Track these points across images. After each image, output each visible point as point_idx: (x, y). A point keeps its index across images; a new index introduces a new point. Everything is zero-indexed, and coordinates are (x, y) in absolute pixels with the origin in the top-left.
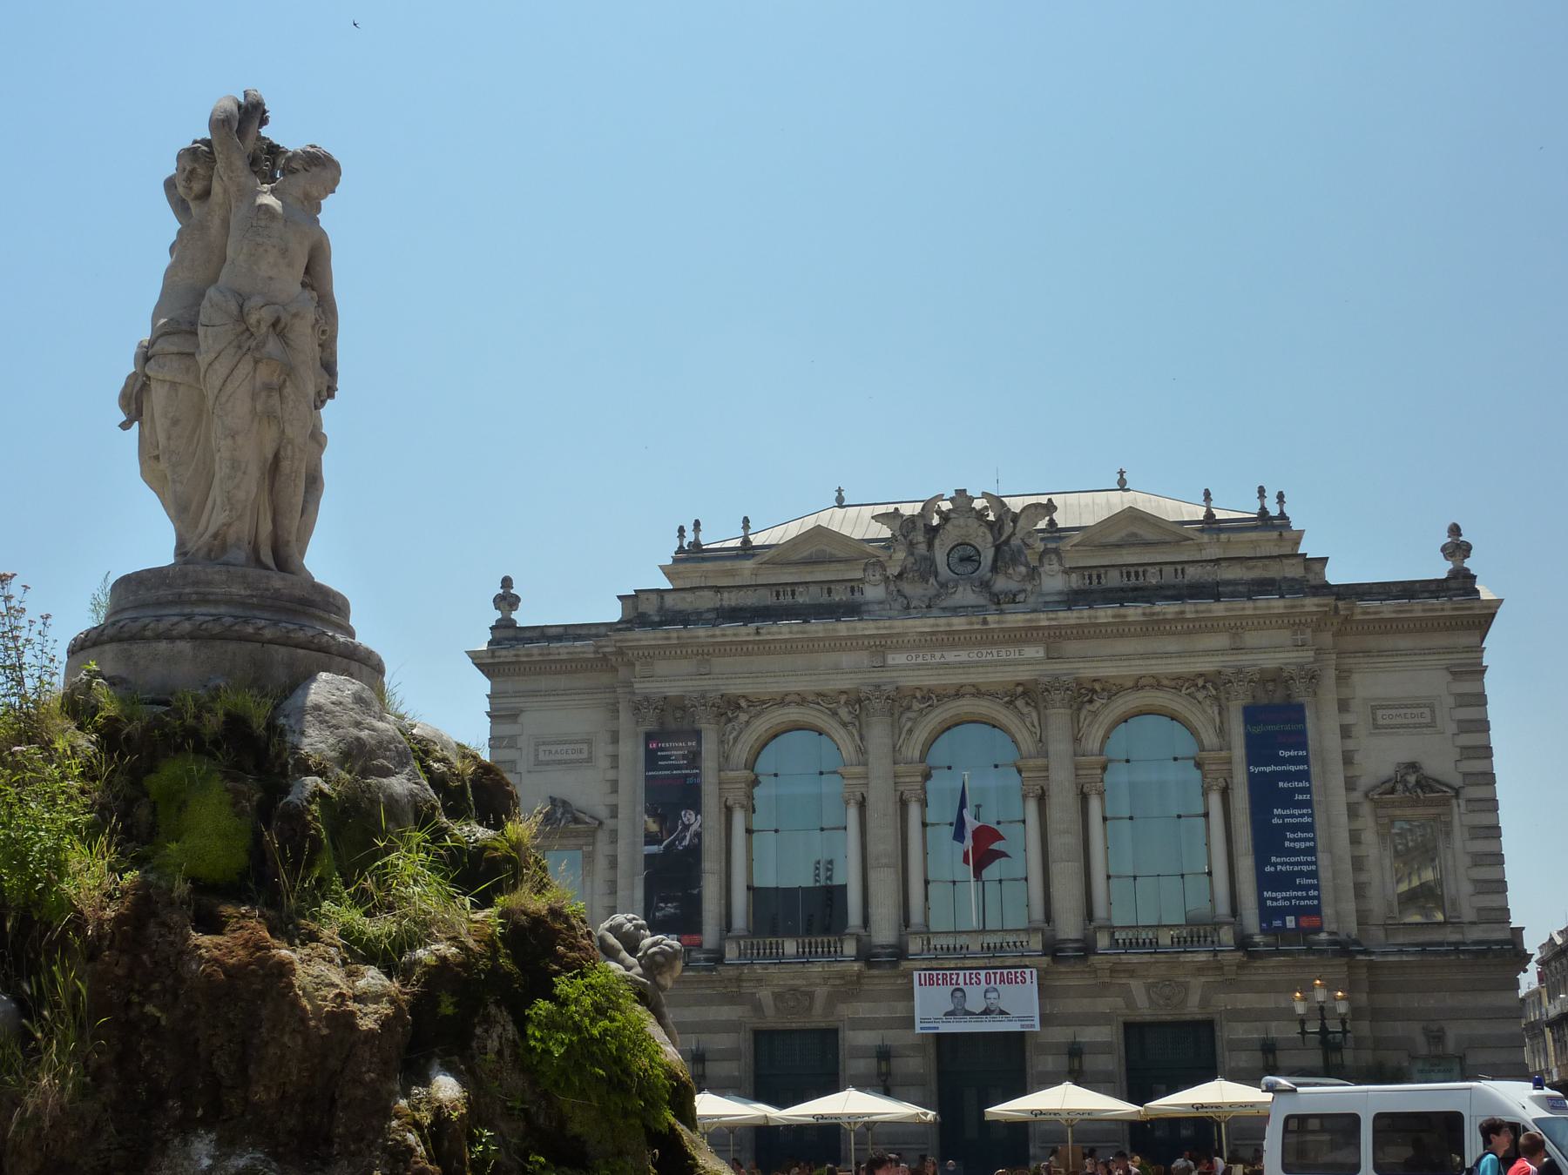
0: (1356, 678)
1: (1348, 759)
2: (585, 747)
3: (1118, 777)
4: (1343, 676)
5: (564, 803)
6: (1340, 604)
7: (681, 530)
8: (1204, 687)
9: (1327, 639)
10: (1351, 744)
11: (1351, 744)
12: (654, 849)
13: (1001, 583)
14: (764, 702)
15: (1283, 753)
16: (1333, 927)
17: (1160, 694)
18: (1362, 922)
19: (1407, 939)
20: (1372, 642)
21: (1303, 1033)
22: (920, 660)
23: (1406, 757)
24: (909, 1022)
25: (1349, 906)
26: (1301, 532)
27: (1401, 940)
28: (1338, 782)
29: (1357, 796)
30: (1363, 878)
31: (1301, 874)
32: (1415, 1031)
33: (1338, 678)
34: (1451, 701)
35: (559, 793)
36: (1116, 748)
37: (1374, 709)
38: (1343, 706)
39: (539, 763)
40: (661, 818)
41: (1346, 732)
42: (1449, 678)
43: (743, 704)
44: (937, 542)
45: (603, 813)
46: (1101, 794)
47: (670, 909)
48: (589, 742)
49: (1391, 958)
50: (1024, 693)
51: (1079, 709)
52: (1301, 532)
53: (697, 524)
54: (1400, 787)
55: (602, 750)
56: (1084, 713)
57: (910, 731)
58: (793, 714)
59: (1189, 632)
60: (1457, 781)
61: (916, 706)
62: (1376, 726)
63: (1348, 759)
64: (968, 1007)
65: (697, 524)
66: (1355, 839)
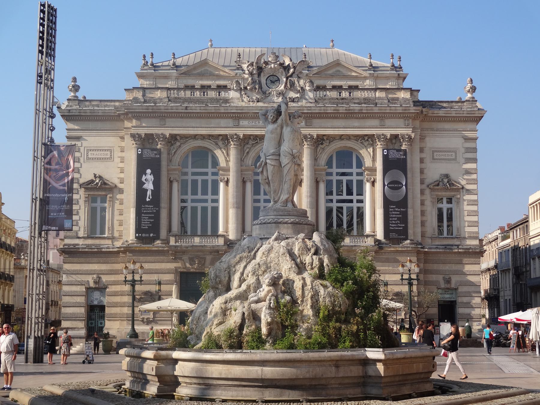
0: (427, 139)
1: (422, 172)
2: (109, 152)
4: (422, 138)
5: (100, 177)
6: (424, 110)
7: (144, 56)
8: (367, 140)
10: (423, 166)
11: (423, 166)
14: (187, 138)
16: (412, 238)
17: (350, 142)
18: (423, 235)
19: (439, 243)
20: (435, 125)
21: (402, 279)
22: (254, 124)
23: (444, 172)
25: (419, 230)
26: (407, 74)
27: (437, 243)
28: (418, 181)
29: (424, 186)
30: (424, 218)
32: (440, 278)
33: (420, 139)
34: (463, 150)
37: (433, 152)
38: (422, 150)
39: (88, 159)
41: (422, 161)
42: (464, 141)
43: (178, 138)
44: (262, 74)
45: (116, 181)
48: (111, 151)
49: (433, 250)
51: (317, 147)
52: (407, 74)
53: (152, 55)
54: (441, 184)
56: (319, 148)
57: (248, 153)
59: (363, 118)
62: (433, 159)
63: (422, 172)
65: (152, 55)
66: (422, 203)
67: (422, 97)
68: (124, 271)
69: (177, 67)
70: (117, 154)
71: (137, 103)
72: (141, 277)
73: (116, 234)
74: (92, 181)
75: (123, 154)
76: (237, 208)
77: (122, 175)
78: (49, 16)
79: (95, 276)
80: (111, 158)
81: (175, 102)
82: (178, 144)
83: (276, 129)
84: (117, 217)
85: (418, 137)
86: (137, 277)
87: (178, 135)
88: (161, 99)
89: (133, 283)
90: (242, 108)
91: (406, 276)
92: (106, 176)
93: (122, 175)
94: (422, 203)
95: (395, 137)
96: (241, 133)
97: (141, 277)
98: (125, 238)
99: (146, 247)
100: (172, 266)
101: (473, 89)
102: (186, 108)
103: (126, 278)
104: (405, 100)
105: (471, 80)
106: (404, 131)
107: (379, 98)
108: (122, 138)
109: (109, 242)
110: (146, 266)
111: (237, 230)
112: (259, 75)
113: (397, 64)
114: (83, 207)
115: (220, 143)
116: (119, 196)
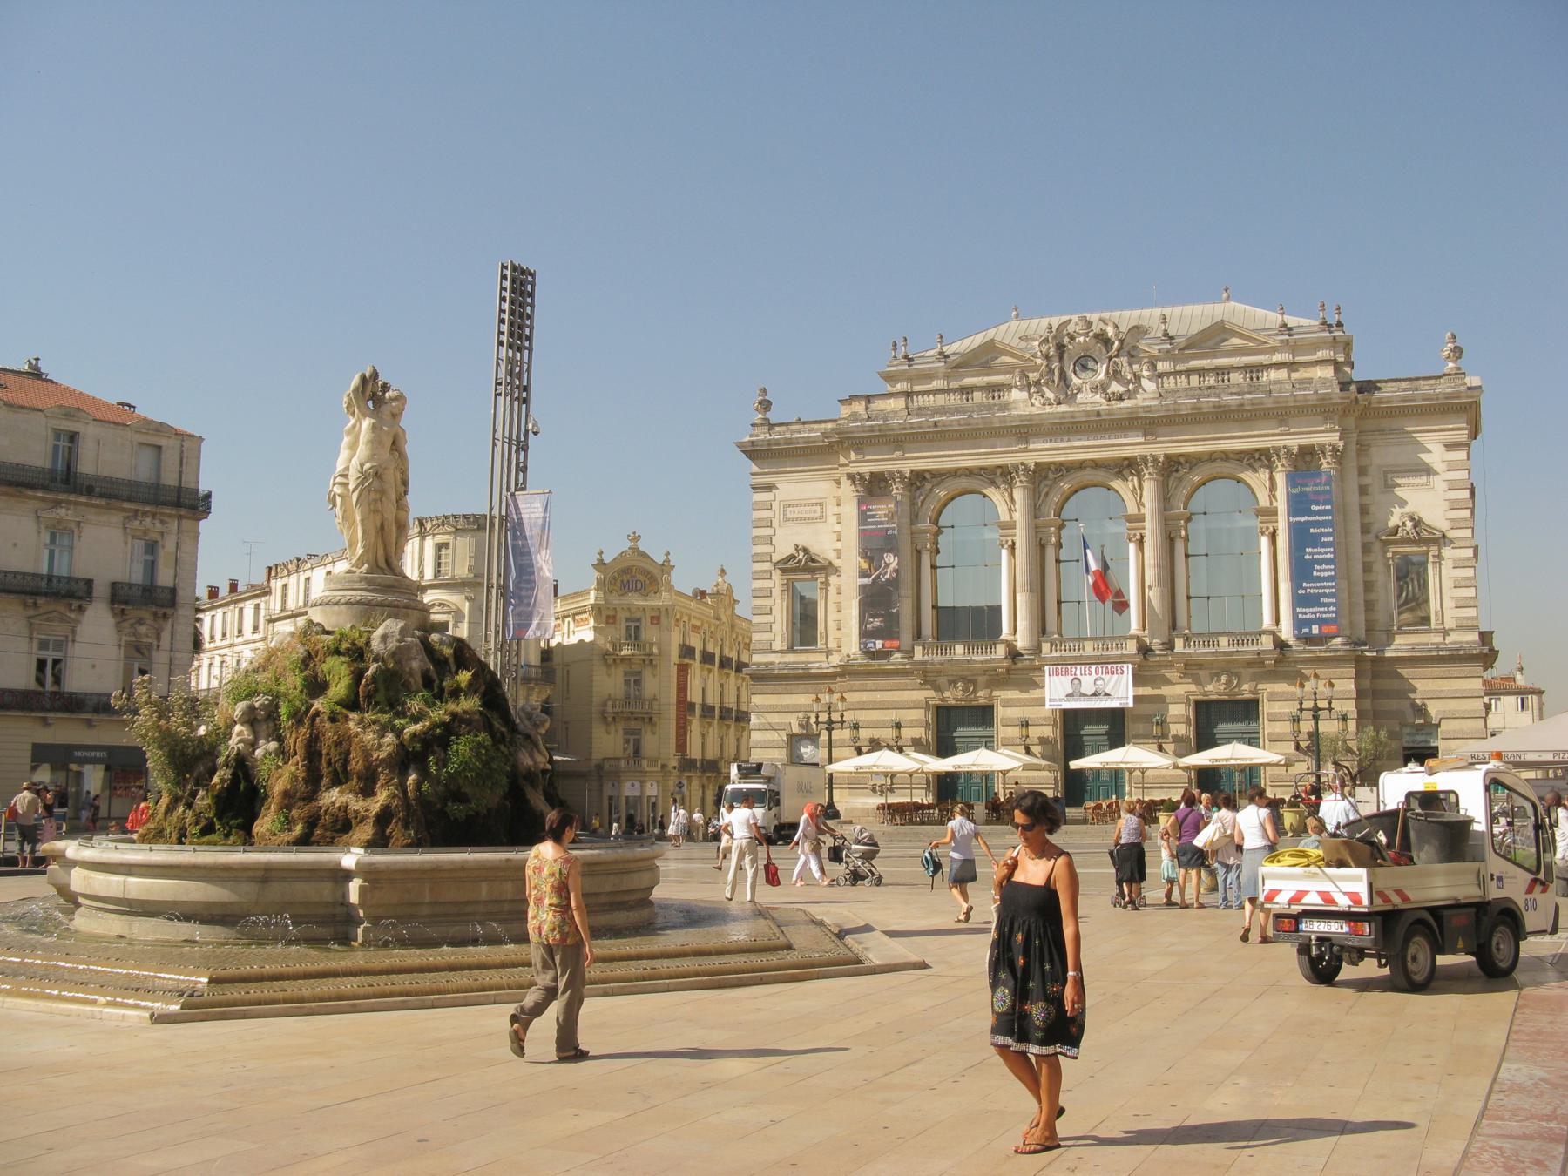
0: (1373, 450)
1: (1364, 510)
3: (1198, 526)
4: (1362, 449)
5: (805, 550)
9: (1351, 422)
10: (1367, 500)
11: (1367, 500)
12: (866, 581)
13: (1115, 387)
15: (1314, 508)
20: (1385, 423)
21: (1301, 710)
24: (1040, 703)
30: (1373, 596)
31: (1325, 595)
35: (801, 544)
36: (1196, 504)
37: (1386, 473)
38: (1362, 471)
39: (786, 520)
40: (870, 559)
41: (1363, 490)
43: (928, 476)
45: (831, 556)
46: (1186, 539)
47: (877, 623)
48: (821, 505)
58: (964, 483)
59: (1248, 419)
60: (1444, 525)
61: (1051, 476)
63: (1364, 510)
64: (1083, 690)
69: (947, 356)
70: (831, 509)
73: (832, 645)
74: (793, 557)
76: (1031, 591)
77: (839, 545)
79: (801, 715)
80: (822, 517)
81: (918, 415)
82: (928, 486)
84: (832, 616)
85: (1353, 447)
86: (836, 717)
88: (895, 412)
90: (1031, 417)
91: (1308, 704)
92: (814, 549)
93: (839, 545)
94: (1367, 568)
95: (1307, 453)
96: (1031, 460)
98: (845, 651)
99: (876, 664)
100: (921, 695)
101: (1458, 352)
102: (936, 424)
104: (1324, 381)
105: (1454, 337)
106: (1324, 436)
107: (1277, 382)
108: (838, 482)
109: (822, 657)
110: (852, 697)
111: (1032, 629)
112: (1061, 359)
113: (1333, 320)
114: (779, 601)
115: (999, 481)
116: (833, 579)
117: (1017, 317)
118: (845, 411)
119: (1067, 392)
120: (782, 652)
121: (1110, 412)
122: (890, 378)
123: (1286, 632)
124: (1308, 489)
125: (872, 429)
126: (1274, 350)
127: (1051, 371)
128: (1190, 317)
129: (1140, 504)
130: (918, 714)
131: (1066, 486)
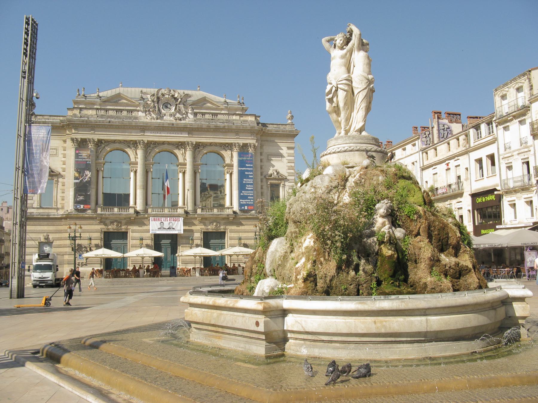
0: (264, 147)
2: (55, 151)
4: (262, 146)
9: (259, 136)
10: (262, 164)
11: (262, 164)
12: (77, 181)
15: (247, 165)
20: (269, 138)
21: (256, 235)
24: (148, 231)
29: (263, 177)
31: (249, 196)
38: (261, 154)
40: (79, 173)
43: (103, 142)
44: (160, 102)
45: (60, 171)
47: (81, 198)
48: (56, 150)
50: (181, 145)
51: (195, 150)
55: (61, 151)
57: (150, 153)
58: (117, 146)
61: (152, 146)
64: (164, 227)
67: (261, 120)
68: (69, 230)
69: (100, 97)
70: (61, 151)
71: (76, 117)
72: (80, 235)
73: (59, 206)
75: (65, 152)
77: (64, 166)
78: (33, 29)
79: (45, 234)
81: (102, 118)
82: (103, 146)
83: (346, 54)
86: (78, 235)
87: (103, 140)
88: (92, 116)
89: (74, 239)
90: (147, 123)
93: (64, 166)
95: (245, 146)
96: (146, 139)
97: (80, 235)
98: (66, 209)
99: (81, 214)
101: (292, 117)
102: (109, 122)
103: (70, 235)
104: (252, 121)
106: (251, 141)
107: (235, 120)
108: (65, 141)
109: (55, 211)
110: (84, 227)
112: (158, 103)
115: (131, 146)
116: (60, 180)
117: (122, 86)
118: (70, 113)
119: (160, 116)
120: (37, 208)
121: (177, 124)
122: (76, 103)
123: (236, 208)
124: (245, 158)
125: (83, 121)
126: (222, 109)
127: (155, 107)
128: (196, 94)
129: (185, 159)
130: (98, 235)
131: (157, 150)
